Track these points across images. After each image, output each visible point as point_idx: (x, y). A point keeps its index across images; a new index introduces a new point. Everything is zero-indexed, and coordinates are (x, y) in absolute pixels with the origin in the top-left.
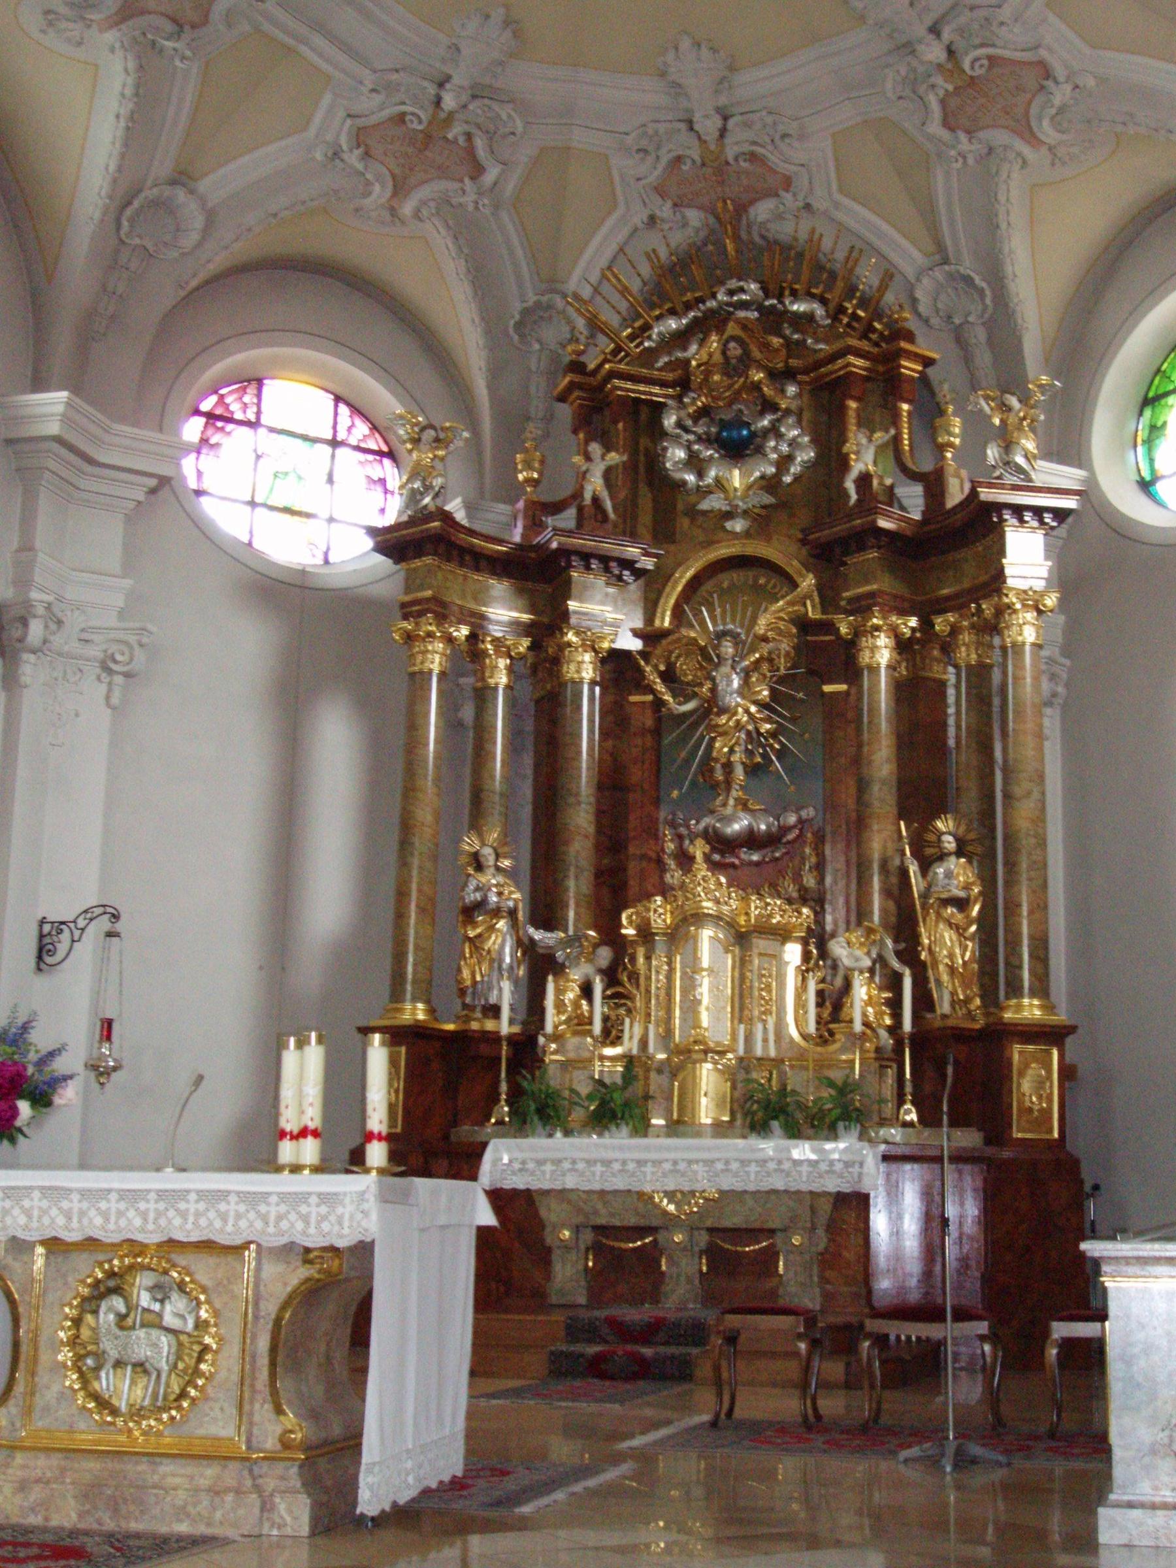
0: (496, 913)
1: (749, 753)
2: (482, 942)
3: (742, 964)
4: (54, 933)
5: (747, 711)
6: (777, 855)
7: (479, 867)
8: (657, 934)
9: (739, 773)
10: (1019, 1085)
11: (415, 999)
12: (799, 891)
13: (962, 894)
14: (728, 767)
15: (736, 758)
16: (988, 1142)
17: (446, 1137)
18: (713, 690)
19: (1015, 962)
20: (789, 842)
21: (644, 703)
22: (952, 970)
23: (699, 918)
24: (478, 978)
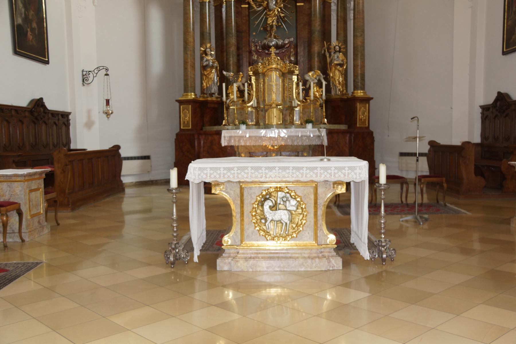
0: (212, 67)
1: (277, 22)
2: (209, 76)
3: (283, 81)
4: (87, 74)
5: (278, 10)
6: (283, 51)
7: (206, 55)
8: (260, 73)
9: (275, 27)
10: (359, 113)
11: (191, 92)
12: (290, 61)
13: (342, 62)
14: (272, 27)
15: (274, 23)
16: (349, 127)
17: (202, 129)
18: (268, 4)
19: (356, 80)
20: (287, 47)
21: (245, 7)
22: (339, 82)
23: (271, 70)
24: (208, 86)
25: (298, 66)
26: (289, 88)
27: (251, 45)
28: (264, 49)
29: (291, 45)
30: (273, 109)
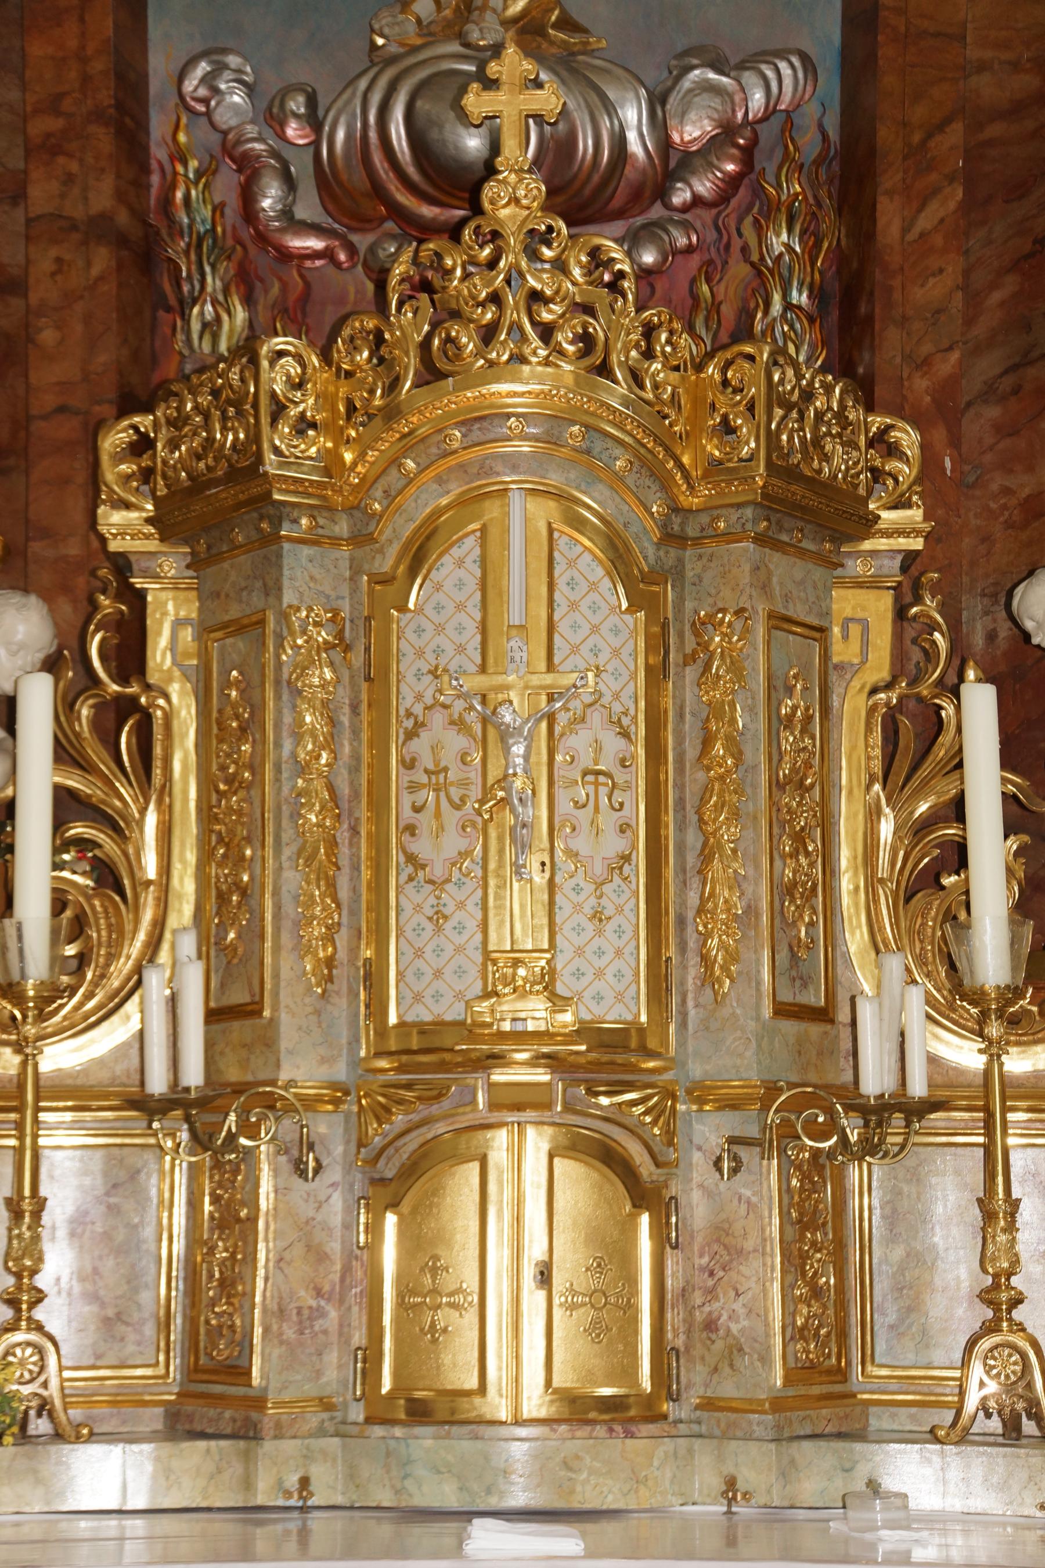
20: (697, 201)
25: (907, 438)
26: (777, 785)
27: (159, 153)
28: (362, 222)
29: (767, 163)
30: (500, 1140)
